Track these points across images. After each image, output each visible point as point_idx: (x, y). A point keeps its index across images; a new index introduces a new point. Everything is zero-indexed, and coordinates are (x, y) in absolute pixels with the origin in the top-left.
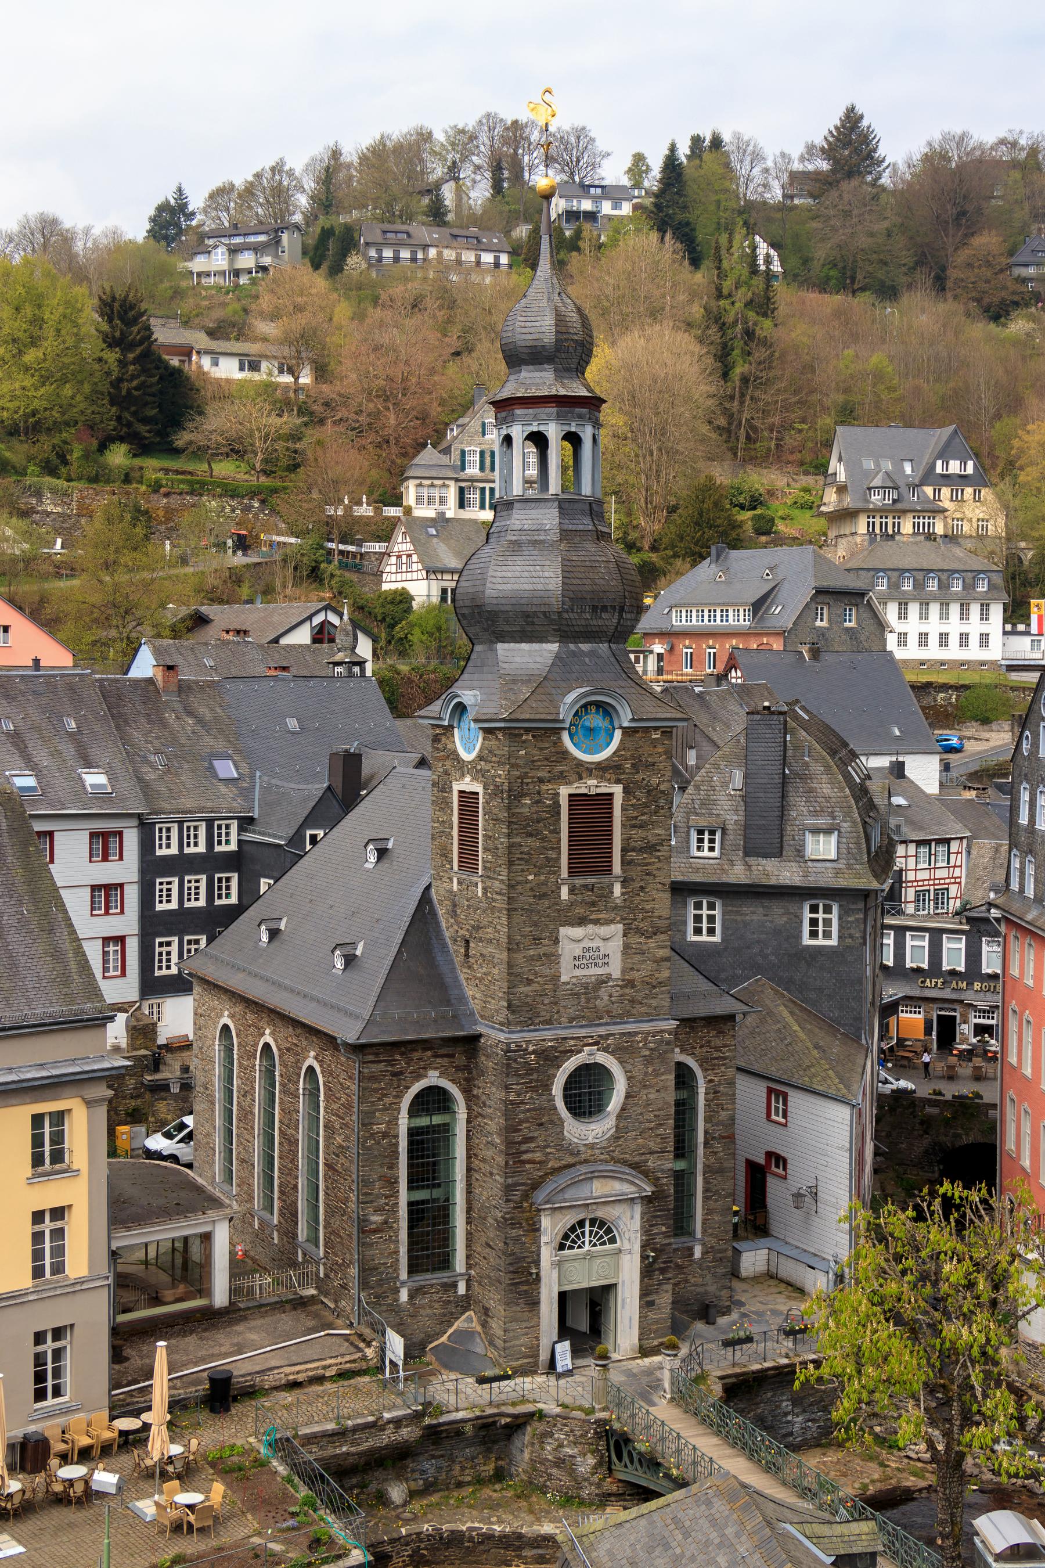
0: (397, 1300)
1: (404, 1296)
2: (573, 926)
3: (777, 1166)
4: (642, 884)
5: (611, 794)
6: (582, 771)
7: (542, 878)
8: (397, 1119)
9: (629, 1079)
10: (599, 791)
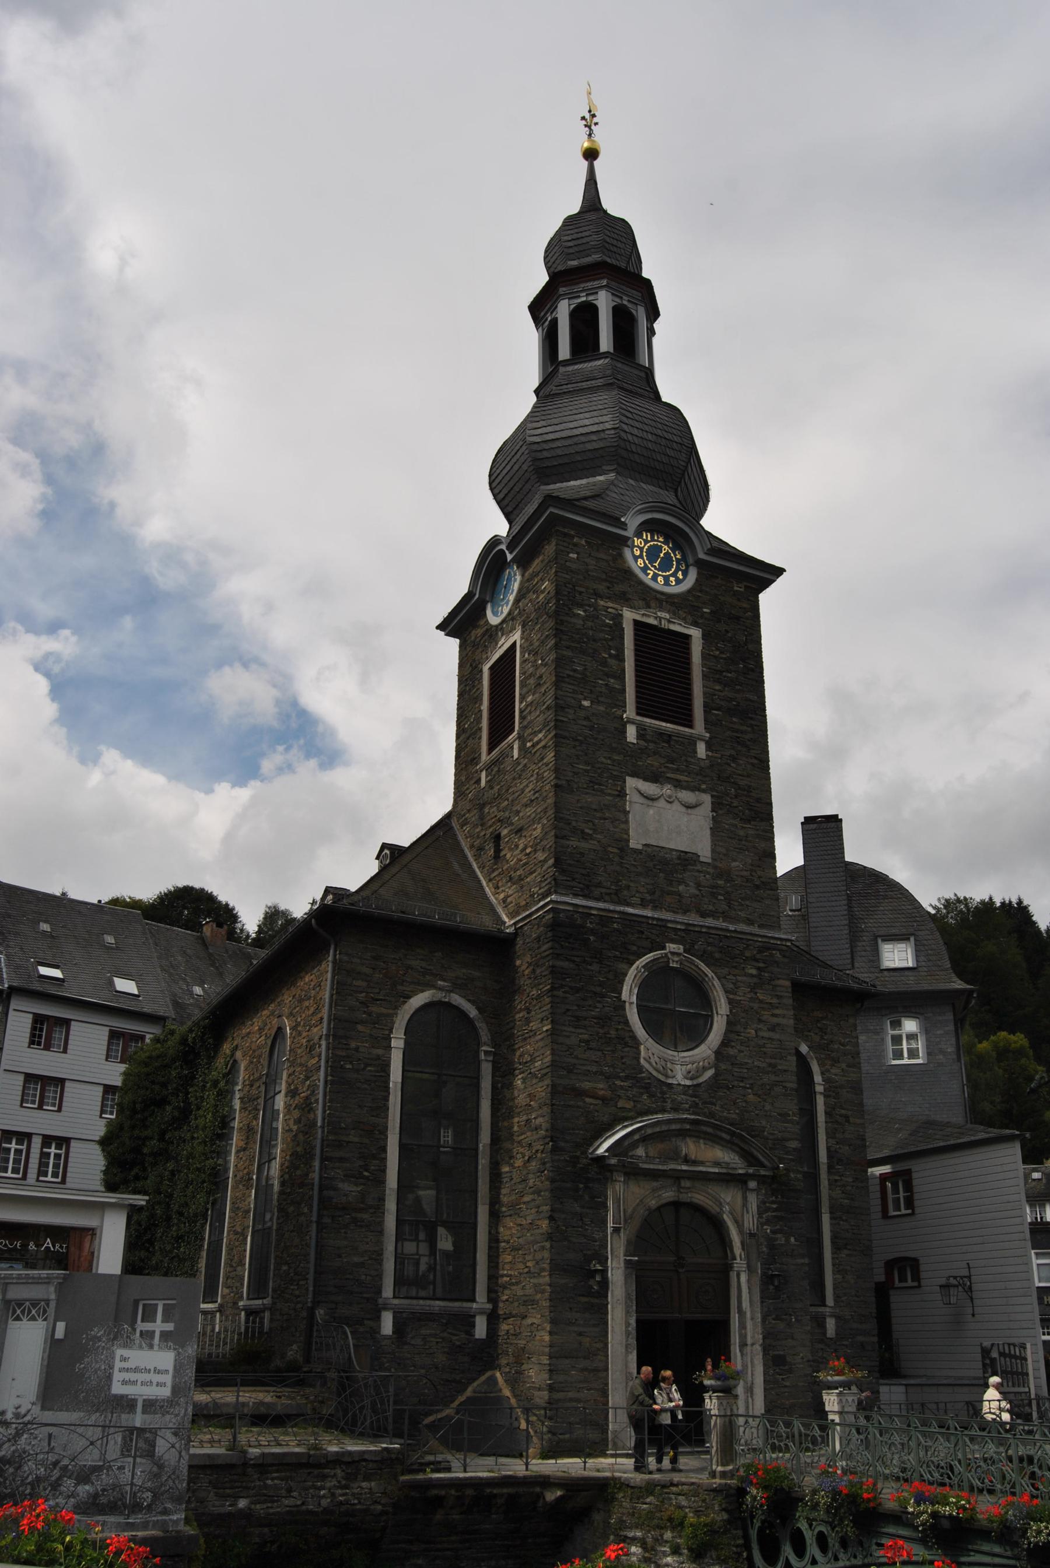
0: (376, 1330)
1: (387, 1325)
2: (645, 779)
3: (903, 1279)
4: (733, 752)
5: (688, 637)
6: (648, 597)
7: (602, 708)
8: (389, 1039)
9: (730, 1002)
10: (673, 627)
